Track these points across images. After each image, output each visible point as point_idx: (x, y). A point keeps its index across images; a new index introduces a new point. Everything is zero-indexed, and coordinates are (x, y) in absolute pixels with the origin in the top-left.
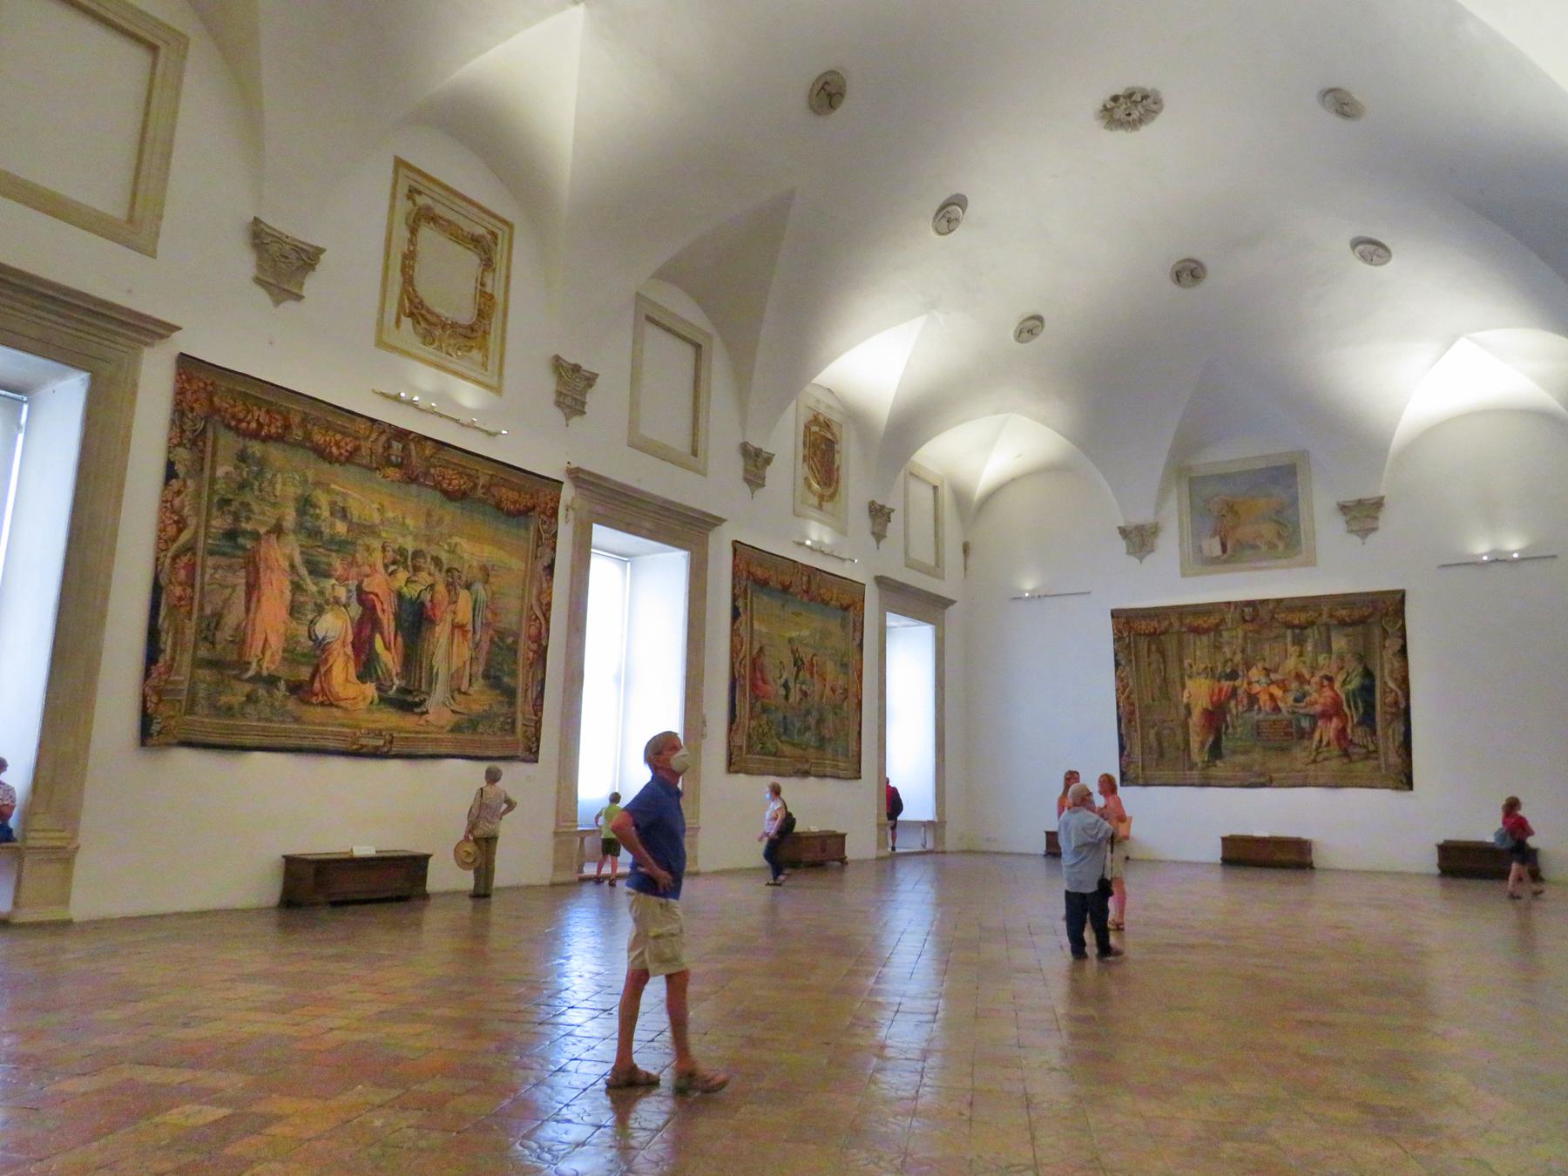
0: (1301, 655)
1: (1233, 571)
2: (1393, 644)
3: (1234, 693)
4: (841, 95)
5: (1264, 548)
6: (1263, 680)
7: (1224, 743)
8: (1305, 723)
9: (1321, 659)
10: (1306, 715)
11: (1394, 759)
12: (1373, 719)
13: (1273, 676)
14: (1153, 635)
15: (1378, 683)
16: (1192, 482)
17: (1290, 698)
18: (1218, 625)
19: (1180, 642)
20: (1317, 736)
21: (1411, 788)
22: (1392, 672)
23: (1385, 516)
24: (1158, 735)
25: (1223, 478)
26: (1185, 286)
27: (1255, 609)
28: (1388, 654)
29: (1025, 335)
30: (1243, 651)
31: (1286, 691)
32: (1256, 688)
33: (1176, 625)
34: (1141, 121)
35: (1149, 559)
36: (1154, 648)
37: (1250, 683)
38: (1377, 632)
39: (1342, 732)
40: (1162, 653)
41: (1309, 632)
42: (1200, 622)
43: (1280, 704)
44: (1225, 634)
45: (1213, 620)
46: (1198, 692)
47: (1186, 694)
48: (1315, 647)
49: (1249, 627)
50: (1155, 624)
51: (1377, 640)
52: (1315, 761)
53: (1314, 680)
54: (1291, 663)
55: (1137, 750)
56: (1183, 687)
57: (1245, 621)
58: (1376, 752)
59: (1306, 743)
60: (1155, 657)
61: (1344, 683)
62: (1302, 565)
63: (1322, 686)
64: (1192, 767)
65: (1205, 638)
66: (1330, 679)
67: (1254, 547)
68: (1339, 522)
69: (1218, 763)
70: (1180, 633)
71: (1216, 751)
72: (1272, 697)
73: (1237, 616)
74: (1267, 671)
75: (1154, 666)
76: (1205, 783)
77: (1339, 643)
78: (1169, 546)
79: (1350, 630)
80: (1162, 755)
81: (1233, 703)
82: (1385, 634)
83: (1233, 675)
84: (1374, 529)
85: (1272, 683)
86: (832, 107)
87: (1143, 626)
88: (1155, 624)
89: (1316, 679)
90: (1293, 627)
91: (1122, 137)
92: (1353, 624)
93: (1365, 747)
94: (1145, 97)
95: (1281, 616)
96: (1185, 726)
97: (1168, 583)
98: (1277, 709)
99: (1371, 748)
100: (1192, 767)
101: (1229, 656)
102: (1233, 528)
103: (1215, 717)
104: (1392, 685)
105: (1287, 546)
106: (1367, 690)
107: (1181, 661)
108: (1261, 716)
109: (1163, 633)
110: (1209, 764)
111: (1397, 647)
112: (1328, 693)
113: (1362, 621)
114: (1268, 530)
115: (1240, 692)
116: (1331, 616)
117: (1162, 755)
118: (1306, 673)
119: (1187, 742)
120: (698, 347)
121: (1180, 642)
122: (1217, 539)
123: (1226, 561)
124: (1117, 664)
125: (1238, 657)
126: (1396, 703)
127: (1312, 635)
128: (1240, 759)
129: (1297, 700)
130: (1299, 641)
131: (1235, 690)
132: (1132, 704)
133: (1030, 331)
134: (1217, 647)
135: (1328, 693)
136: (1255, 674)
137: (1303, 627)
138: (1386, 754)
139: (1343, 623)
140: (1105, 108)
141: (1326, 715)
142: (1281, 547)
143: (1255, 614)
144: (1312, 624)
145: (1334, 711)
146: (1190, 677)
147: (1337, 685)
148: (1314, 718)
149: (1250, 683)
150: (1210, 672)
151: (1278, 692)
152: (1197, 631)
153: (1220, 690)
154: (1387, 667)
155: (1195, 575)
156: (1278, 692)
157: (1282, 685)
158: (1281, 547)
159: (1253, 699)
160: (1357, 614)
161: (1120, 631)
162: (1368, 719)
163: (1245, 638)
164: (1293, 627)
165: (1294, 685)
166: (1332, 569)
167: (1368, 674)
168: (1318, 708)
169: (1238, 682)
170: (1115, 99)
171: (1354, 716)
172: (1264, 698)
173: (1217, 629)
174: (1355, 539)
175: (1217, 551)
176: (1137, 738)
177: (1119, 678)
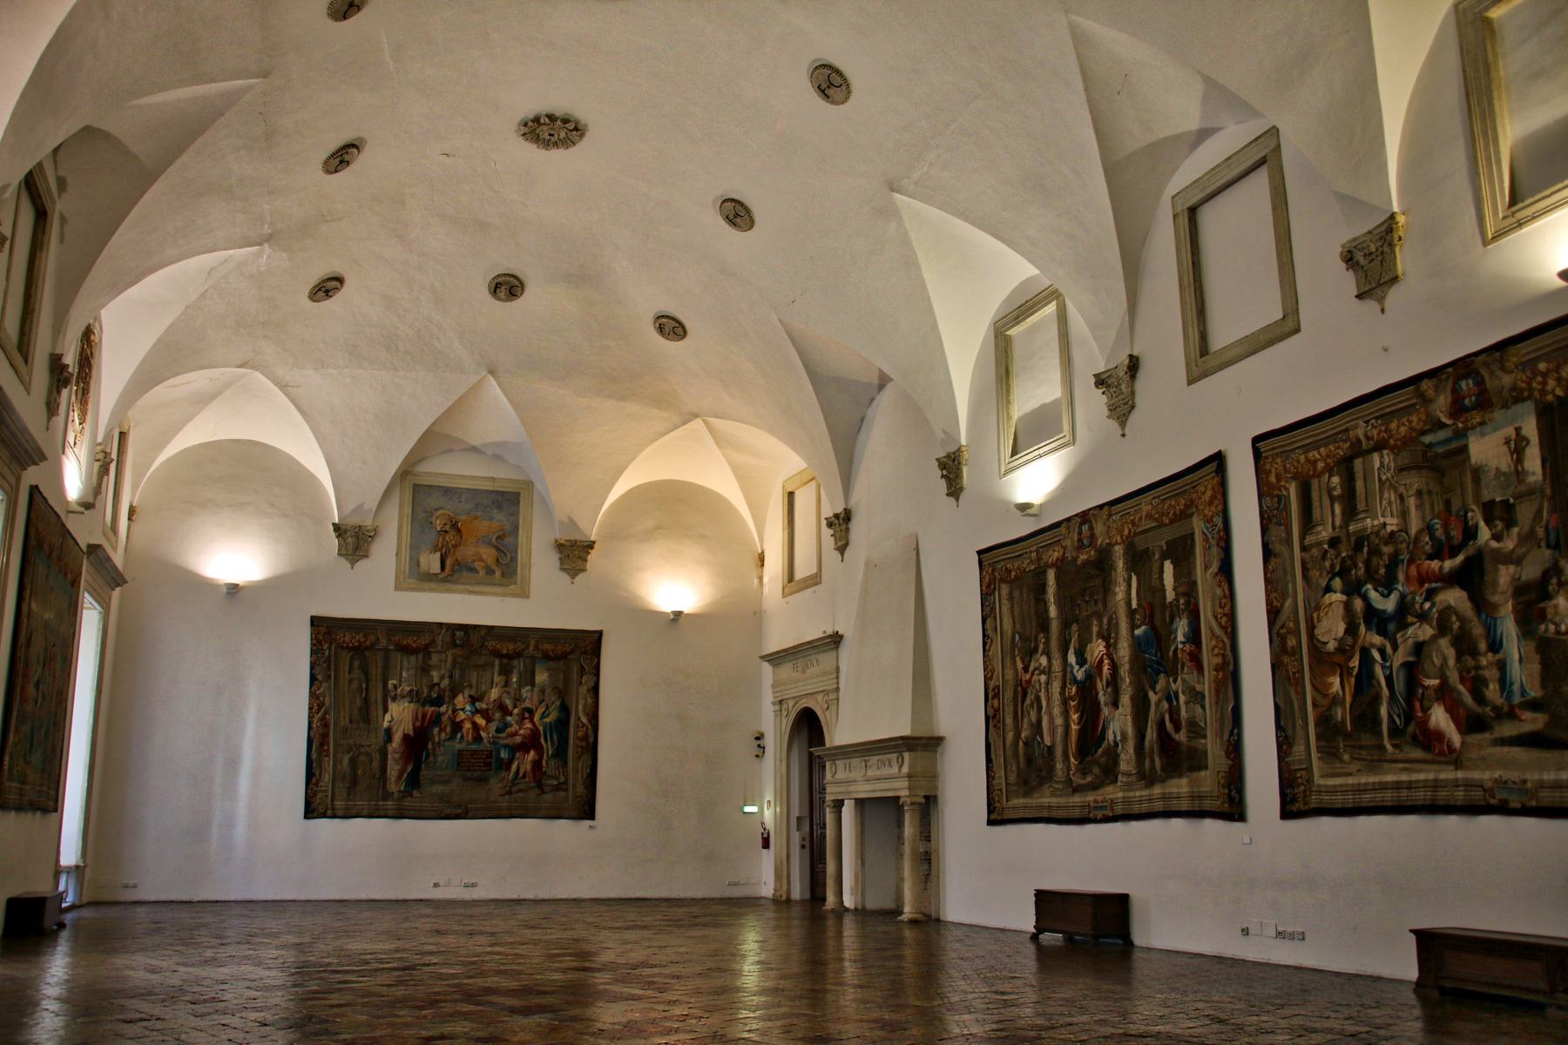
0: (507, 684)
1: (448, 591)
2: (588, 680)
3: (437, 720)
4: (359, 9)
5: (482, 573)
6: (468, 708)
7: (423, 773)
8: (504, 755)
9: (525, 692)
10: (506, 746)
11: (581, 790)
12: (566, 751)
13: (481, 705)
14: (358, 651)
15: (572, 721)
16: (417, 488)
17: (493, 726)
18: (427, 646)
19: (386, 659)
20: (514, 767)
21: (593, 818)
22: (585, 706)
23: (593, 556)
24: (352, 760)
25: (447, 491)
26: (499, 299)
27: (467, 634)
28: (584, 689)
29: (321, 294)
30: (451, 676)
31: (489, 720)
32: (461, 716)
33: (383, 642)
34: (556, 144)
35: (361, 564)
36: (357, 663)
37: (455, 711)
38: (575, 669)
39: (537, 764)
40: (365, 669)
41: (515, 662)
42: (410, 641)
43: (483, 734)
44: (435, 659)
45: (424, 640)
46: (399, 715)
47: (388, 717)
48: (519, 679)
49: (458, 651)
50: (361, 637)
51: (575, 677)
52: (510, 793)
53: (516, 711)
54: (494, 694)
55: (327, 777)
56: (386, 710)
57: (455, 645)
58: (566, 783)
59: (503, 774)
60: (357, 673)
61: (543, 716)
62: (515, 595)
63: (523, 719)
64: (387, 796)
65: (413, 659)
66: (531, 712)
67: (473, 570)
68: (553, 558)
69: (416, 793)
70: (387, 651)
71: (414, 781)
72: (475, 724)
73: (448, 639)
74: (473, 700)
75: (355, 686)
76: (400, 815)
77: (541, 677)
78: (386, 554)
79: (552, 664)
80: (355, 782)
81: (436, 730)
82: (582, 669)
83: (438, 702)
84: (584, 570)
85: (477, 711)
86: (345, 18)
87: (347, 638)
88: (361, 637)
89: (516, 711)
90: (501, 656)
91: (531, 151)
92: (557, 658)
93: (557, 778)
94: (576, 129)
95: (491, 644)
96: (384, 753)
97: (380, 594)
98: (478, 739)
99: (562, 779)
100: (387, 796)
101: (436, 680)
102: (455, 547)
103: (417, 744)
104: (584, 720)
105: (503, 575)
106: (562, 724)
107: (385, 684)
108: (462, 746)
109: (367, 648)
110: (407, 794)
111: (592, 684)
112: (528, 725)
113: (564, 656)
114: (488, 554)
115: (445, 718)
116: (537, 648)
117: (355, 782)
118: (508, 702)
119: (384, 769)
120: (41, 216)
121: (386, 659)
122: (438, 555)
123: (444, 581)
124: (313, 679)
125: (445, 683)
126: (585, 738)
127: (520, 665)
128: (438, 789)
129: (498, 731)
130: (506, 672)
131: (440, 715)
132: (326, 725)
133: (327, 292)
134: (425, 669)
135: (528, 725)
136: (460, 700)
137: (510, 657)
138: (574, 786)
139: (547, 657)
140: (537, 120)
141: (524, 747)
142: (498, 574)
143: (467, 638)
144: (518, 655)
145: (532, 742)
146: (394, 699)
147: (536, 718)
148: (513, 749)
149: (455, 711)
150: (414, 696)
151: (481, 721)
152: (407, 650)
153: (424, 716)
154: (581, 702)
155: (412, 589)
156: (481, 721)
157: (486, 715)
158: (498, 574)
159: (457, 727)
160: (560, 649)
161: (320, 642)
162: (561, 752)
163: (454, 662)
164: (501, 656)
165: (498, 715)
166: (540, 604)
167: (565, 709)
168: (518, 739)
169: (443, 709)
170: (551, 117)
171: (548, 748)
172: (468, 725)
173: (426, 650)
174: (565, 577)
175: (436, 568)
176: (329, 765)
177: (312, 695)
